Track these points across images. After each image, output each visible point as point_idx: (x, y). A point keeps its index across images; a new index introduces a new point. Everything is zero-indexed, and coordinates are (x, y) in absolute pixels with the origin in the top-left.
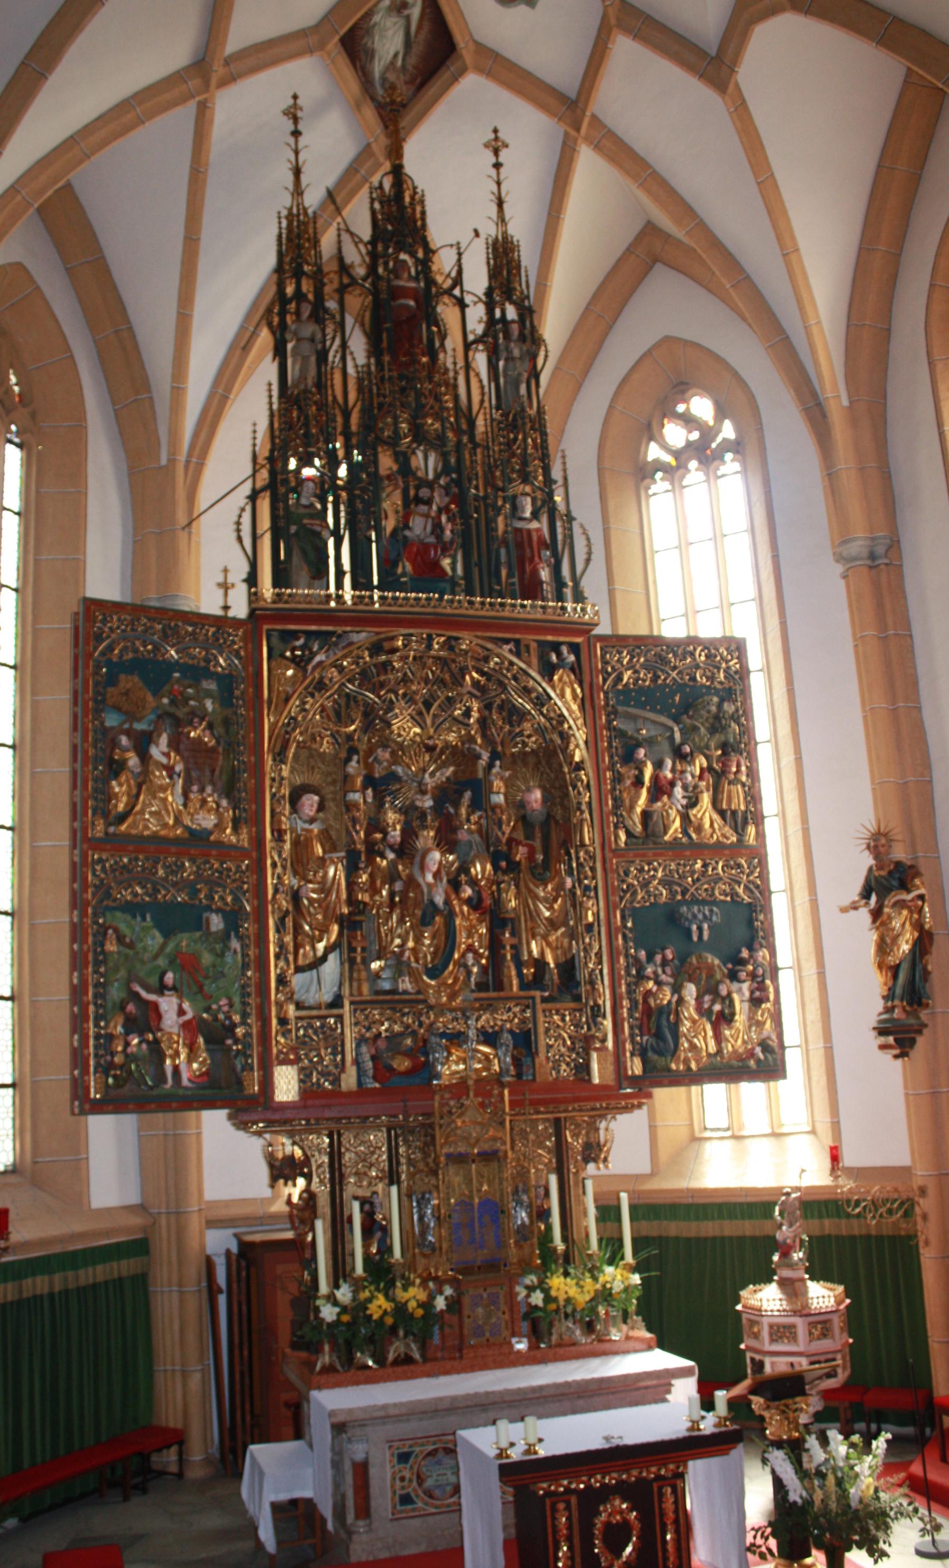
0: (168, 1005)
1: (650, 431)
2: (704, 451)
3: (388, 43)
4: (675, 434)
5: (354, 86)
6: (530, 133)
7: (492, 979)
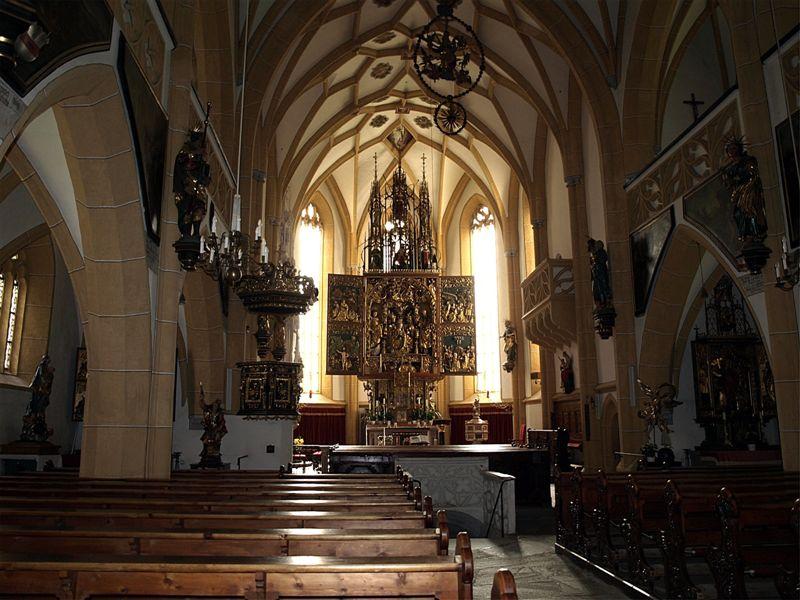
0: (344, 354)
1: (474, 216)
2: (485, 222)
3: (398, 137)
4: (480, 217)
5: (391, 146)
6: (431, 154)
7: (413, 351)
